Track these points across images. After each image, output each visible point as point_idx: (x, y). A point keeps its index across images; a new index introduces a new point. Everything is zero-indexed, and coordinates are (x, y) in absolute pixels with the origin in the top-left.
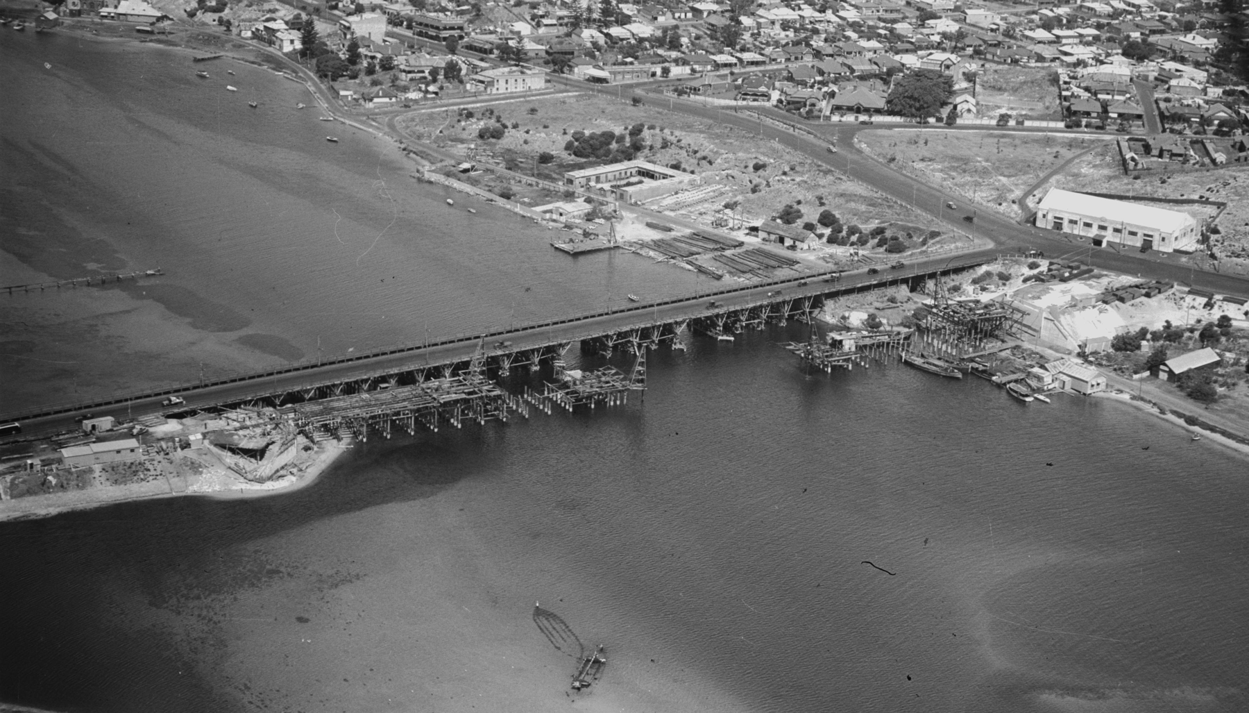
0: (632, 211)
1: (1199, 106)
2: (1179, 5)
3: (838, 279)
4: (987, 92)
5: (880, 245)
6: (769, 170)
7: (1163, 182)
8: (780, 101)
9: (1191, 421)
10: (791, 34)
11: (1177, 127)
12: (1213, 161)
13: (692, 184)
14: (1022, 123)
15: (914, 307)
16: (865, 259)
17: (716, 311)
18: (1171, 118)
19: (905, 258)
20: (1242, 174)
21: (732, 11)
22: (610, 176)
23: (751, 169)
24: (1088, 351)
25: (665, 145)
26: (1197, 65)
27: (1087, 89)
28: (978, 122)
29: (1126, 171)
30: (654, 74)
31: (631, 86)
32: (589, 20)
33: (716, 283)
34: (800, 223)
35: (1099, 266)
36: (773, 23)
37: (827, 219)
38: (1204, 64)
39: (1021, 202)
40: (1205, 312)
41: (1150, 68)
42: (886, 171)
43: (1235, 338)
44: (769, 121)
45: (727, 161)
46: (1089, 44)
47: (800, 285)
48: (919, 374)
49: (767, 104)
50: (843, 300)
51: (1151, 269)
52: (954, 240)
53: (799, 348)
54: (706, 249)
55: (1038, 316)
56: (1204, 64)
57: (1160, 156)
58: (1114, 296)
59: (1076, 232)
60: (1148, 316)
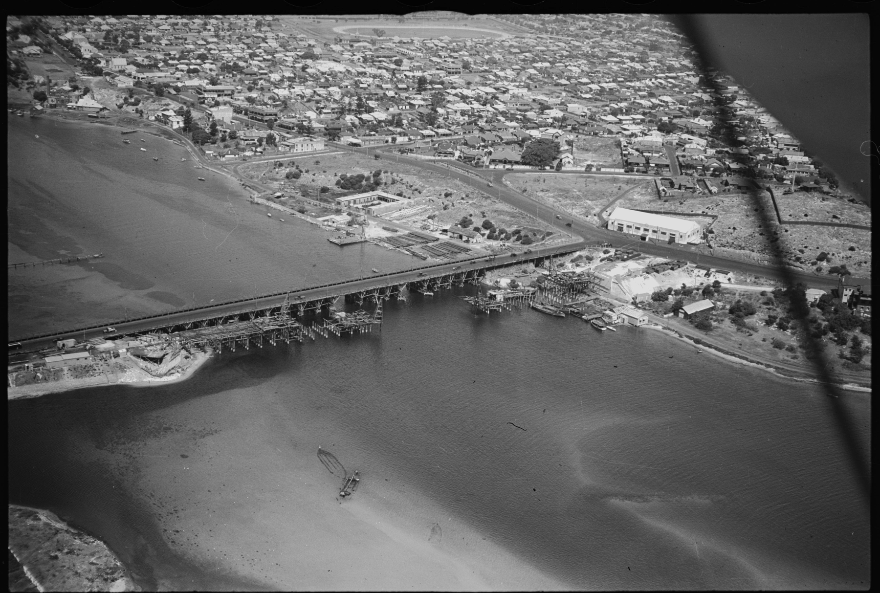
0: (375, 220)
1: (702, 160)
2: (690, 101)
3: (494, 259)
4: (580, 151)
5: (517, 240)
6: (453, 197)
7: (681, 204)
8: (460, 157)
9: (697, 341)
10: (466, 118)
11: (689, 172)
12: (710, 191)
13: (409, 204)
14: (600, 170)
15: (537, 275)
16: (509, 248)
17: (423, 278)
18: (686, 167)
19: (532, 247)
20: (726, 199)
21: (432, 105)
22: (362, 200)
23: (443, 196)
24: (637, 301)
25: (394, 182)
26: (701, 136)
27: (637, 150)
28: (574, 169)
29: (660, 197)
30: (387, 141)
31: (374, 148)
32: (349, 110)
33: (423, 262)
34: (471, 227)
35: (644, 252)
36: (456, 112)
37: (487, 225)
38: (705, 135)
39: (599, 215)
40: (705, 279)
41: (674, 138)
42: (521, 197)
43: (723, 294)
44: (453, 169)
45: (429, 191)
46: (638, 124)
47: (471, 263)
48: (540, 315)
49: (453, 159)
50: (496, 272)
51: (674, 254)
52: (560, 237)
53: (471, 300)
54: (417, 242)
55: (609, 281)
56: (705, 135)
57: (680, 188)
58: (653, 269)
59: (631, 232)
60: (672, 281)
